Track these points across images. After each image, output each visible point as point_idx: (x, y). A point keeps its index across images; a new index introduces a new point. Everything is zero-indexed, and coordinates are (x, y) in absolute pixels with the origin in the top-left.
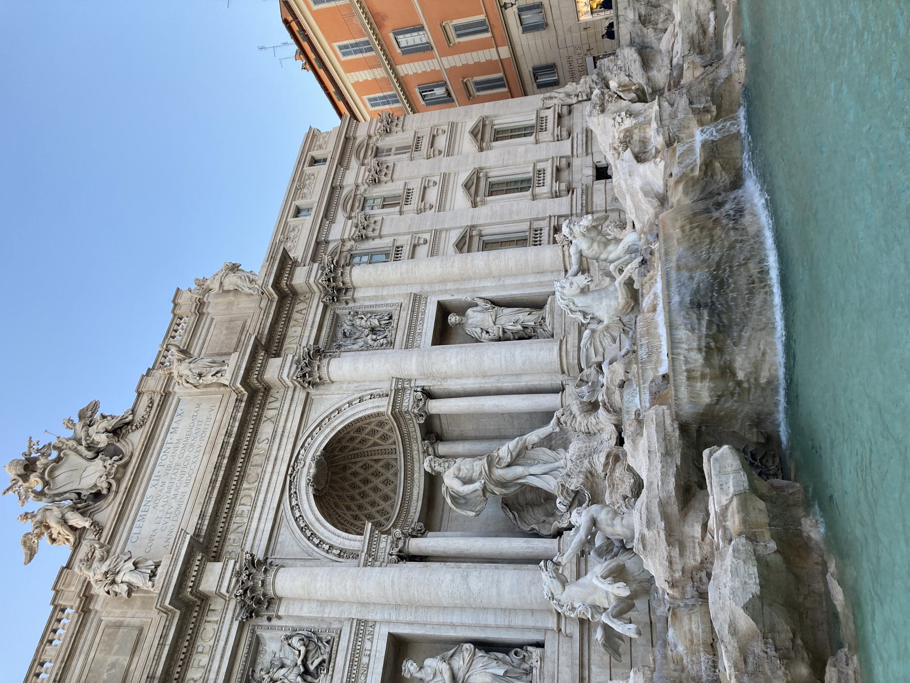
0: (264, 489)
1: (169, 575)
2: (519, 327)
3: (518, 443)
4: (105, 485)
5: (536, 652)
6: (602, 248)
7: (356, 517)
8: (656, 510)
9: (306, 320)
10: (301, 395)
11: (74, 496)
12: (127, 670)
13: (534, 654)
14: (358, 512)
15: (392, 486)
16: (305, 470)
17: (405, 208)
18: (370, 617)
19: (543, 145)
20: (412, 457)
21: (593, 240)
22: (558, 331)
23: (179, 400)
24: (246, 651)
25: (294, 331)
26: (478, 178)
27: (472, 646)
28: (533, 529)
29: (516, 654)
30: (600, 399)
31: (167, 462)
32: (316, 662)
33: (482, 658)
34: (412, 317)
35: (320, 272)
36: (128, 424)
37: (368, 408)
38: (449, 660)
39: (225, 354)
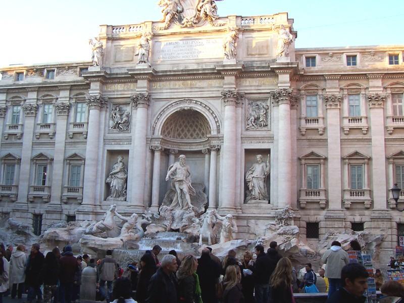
0: (179, 91)
2: (250, 189)
4: (183, 23)
7: (180, 126)
12: (119, 62)
14: (183, 126)
16: (186, 105)
17: (346, 122)
23: (222, 38)
24: (124, 101)
26: (364, 159)
30: (194, 224)
32: (121, 127)
33: (121, 182)
37: (213, 126)
39: (248, 50)
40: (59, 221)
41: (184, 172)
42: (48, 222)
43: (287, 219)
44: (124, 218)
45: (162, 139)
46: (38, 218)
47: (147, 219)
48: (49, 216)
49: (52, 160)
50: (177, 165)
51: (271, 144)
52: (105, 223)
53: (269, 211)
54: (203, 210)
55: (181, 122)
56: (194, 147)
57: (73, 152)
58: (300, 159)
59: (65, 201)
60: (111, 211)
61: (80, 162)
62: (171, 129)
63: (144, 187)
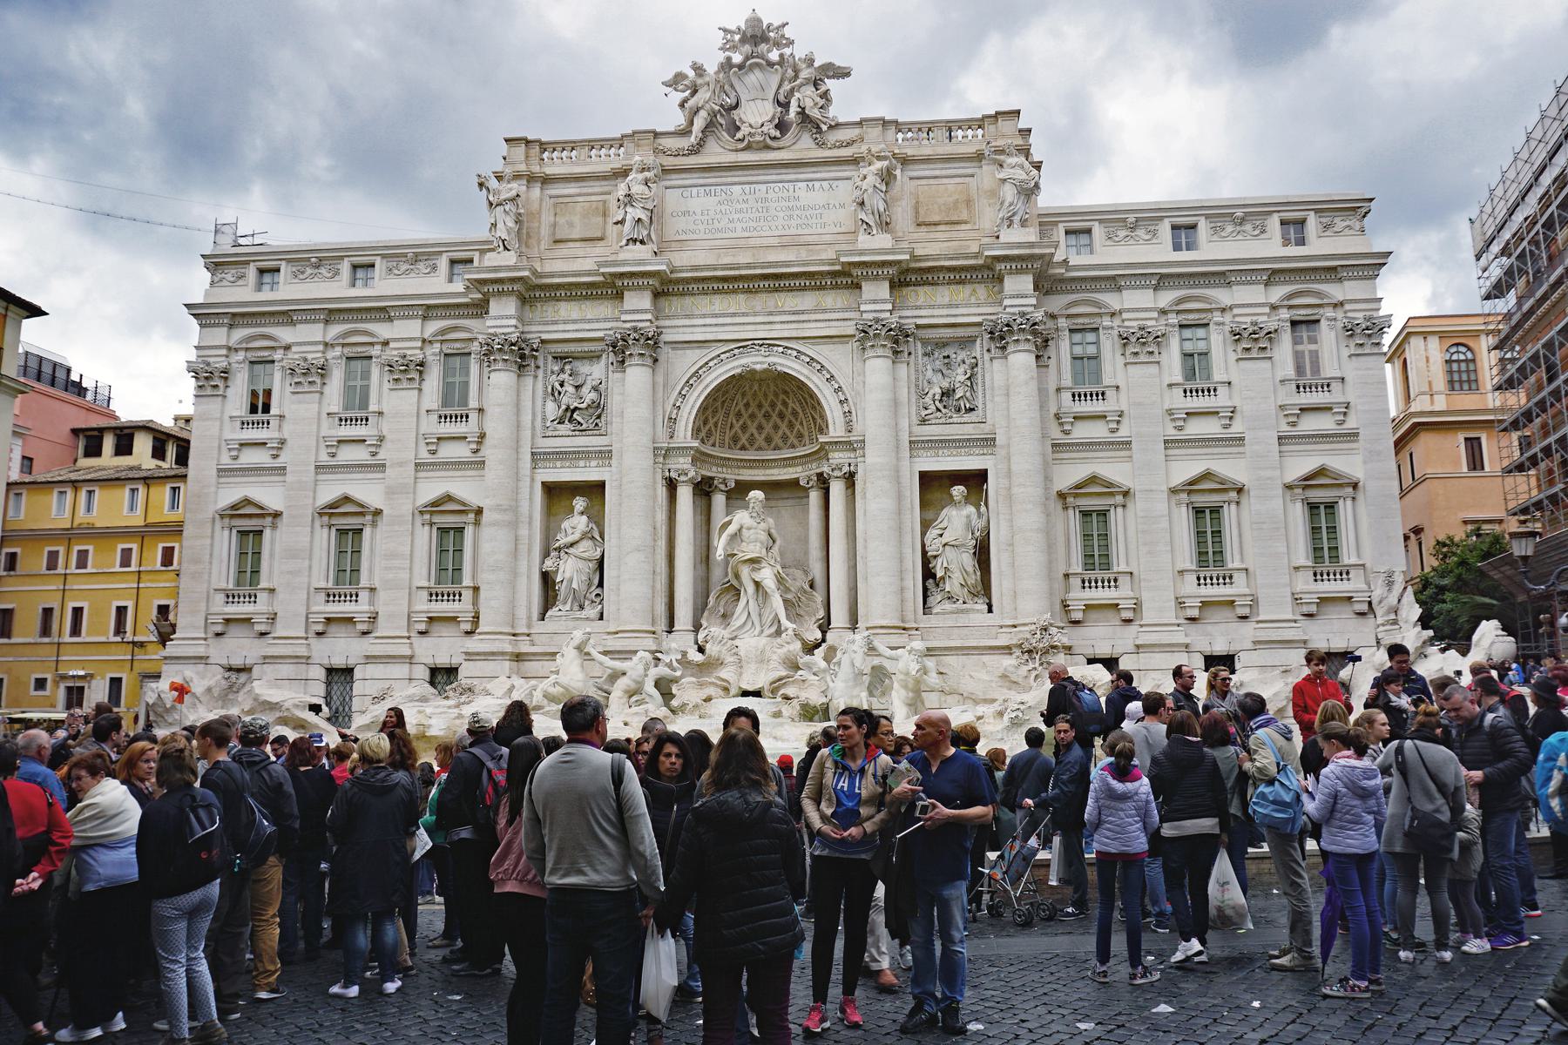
0: (738, 320)
1: (624, 263)
2: (939, 575)
5: (591, 612)
7: (739, 415)
9: (957, 306)
10: (850, 329)
11: (734, 102)
14: (746, 416)
18: (614, 462)
19: (1286, 579)
22: (931, 621)
25: (943, 294)
31: (771, 195)
35: (1016, 310)
36: (818, 127)
41: (764, 537)
42: (373, 689)
43: (1047, 652)
44: (618, 665)
45: (697, 450)
47: (670, 665)
50: (741, 517)
52: (563, 679)
53: (994, 630)
54: (819, 635)
55: (741, 406)
58: (1062, 496)
59: (422, 627)
62: (716, 425)
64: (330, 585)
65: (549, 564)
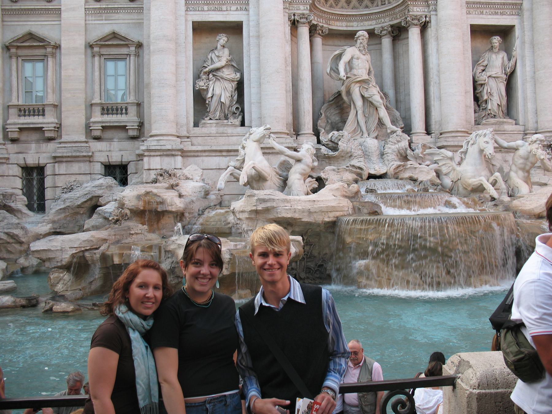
2: (485, 97)
3: (377, 102)
5: (237, 121)
6: (522, 166)
8: (269, 205)
13: (236, 120)
15: (357, 5)
20: (379, 18)
21: (527, 159)
27: (238, 79)
28: (321, 114)
29: (237, 108)
30: (409, 163)
33: (231, 87)
34: (498, 4)
38: (228, 65)
40: (88, 177)
42: (61, 182)
46: (33, 175)
48: (62, 168)
49: (57, 47)
51: (515, 17)
54: (409, 138)
56: (355, 24)
57: (107, 30)
59: (97, 133)
60: (259, 141)
61: (124, 51)
63: (286, 96)
64: (20, 103)
65: (201, 84)
